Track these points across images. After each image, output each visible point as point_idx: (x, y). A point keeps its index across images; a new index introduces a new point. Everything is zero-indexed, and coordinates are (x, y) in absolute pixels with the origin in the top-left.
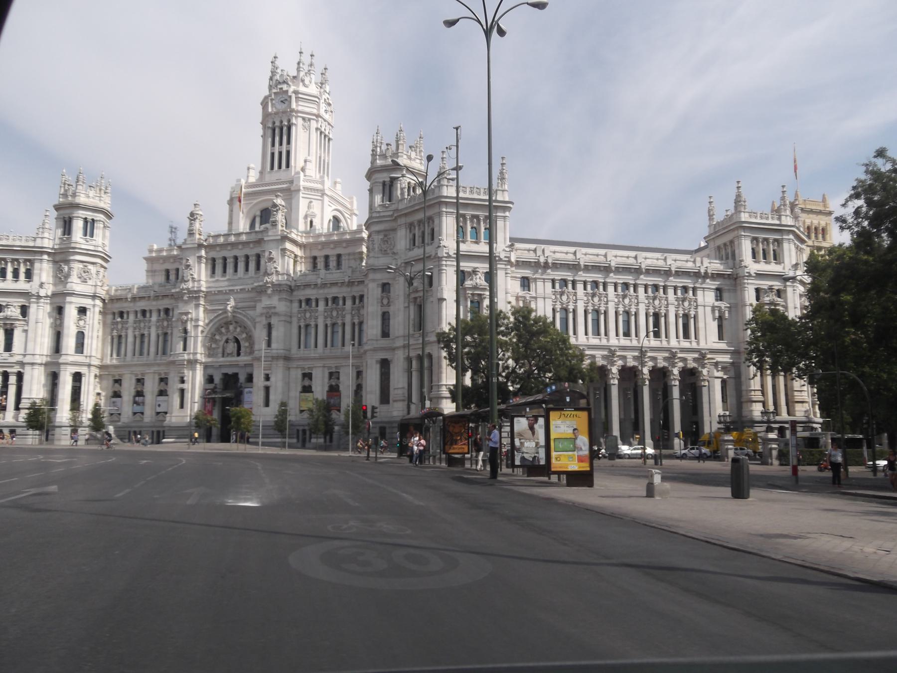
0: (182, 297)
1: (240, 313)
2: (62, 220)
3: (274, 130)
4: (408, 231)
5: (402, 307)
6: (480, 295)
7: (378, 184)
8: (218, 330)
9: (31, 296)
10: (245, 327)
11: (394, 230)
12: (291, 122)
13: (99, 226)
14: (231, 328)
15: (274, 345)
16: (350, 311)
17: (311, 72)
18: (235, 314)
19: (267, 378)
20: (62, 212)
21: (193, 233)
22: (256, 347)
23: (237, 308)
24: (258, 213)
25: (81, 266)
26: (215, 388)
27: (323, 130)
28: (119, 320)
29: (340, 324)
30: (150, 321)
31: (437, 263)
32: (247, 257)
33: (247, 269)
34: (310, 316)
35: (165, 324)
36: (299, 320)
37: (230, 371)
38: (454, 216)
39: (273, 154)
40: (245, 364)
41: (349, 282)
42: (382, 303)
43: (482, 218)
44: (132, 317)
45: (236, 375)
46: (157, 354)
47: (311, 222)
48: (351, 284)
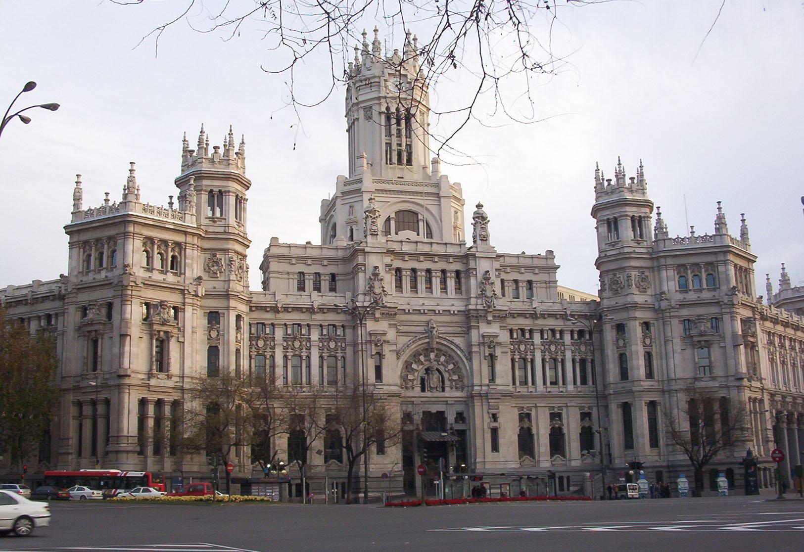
0: (373, 314)
1: (446, 339)
3: (388, 119)
5: (678, 348)
7: (628, 218)
8: (416, 356)
12: (413, 111)
14: (432, 356)
15: (498, 381)
18: (438, 340)
19: (495, 417)
21: (377, 235)
22: (476, 381)
24: (393, 215)
29: (560, 360)
30: (309, 340)
31: (728, 310)
33: (444, 288)
35: (332, 345)
36: (513, 352)
37: (434, 409)
39: (389, 145)
40: (455, 401)
42: (644, 342)
44: (279, 333)
45: (441, 414)
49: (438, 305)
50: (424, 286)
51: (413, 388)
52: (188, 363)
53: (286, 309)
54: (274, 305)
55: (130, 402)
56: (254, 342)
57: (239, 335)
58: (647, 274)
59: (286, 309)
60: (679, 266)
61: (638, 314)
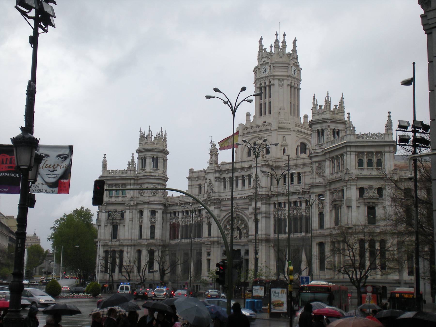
1: (240, 212)
2: (141, 159)
4: (331, 162)
6: (374, 202)
9: (126, 205)
11: (324, 161)
12: (271, 83)
13: (160, 161)
16: (305, 210)
17: (284, 47)
18: (237, 213)
20: (140, 154)
23: (239, 209)
27: (293, 84)
29: (298, 218)
31: (345, 184)
33: (243, 184)
34: (281, 213)
38: (356, 154)
39: (261, 104)
40: (244, 244)
41: (303, 192)
43: (375, 153)
44: (181, 215)
47: (284, 150)
48: (304, 193)
49: (239, 194)
52: (127, 234)
53: (182, 204)
55: (100, 252)
57: (153, 220)
58: (323, 164)
60: (333, 158)
61: (316, 190)
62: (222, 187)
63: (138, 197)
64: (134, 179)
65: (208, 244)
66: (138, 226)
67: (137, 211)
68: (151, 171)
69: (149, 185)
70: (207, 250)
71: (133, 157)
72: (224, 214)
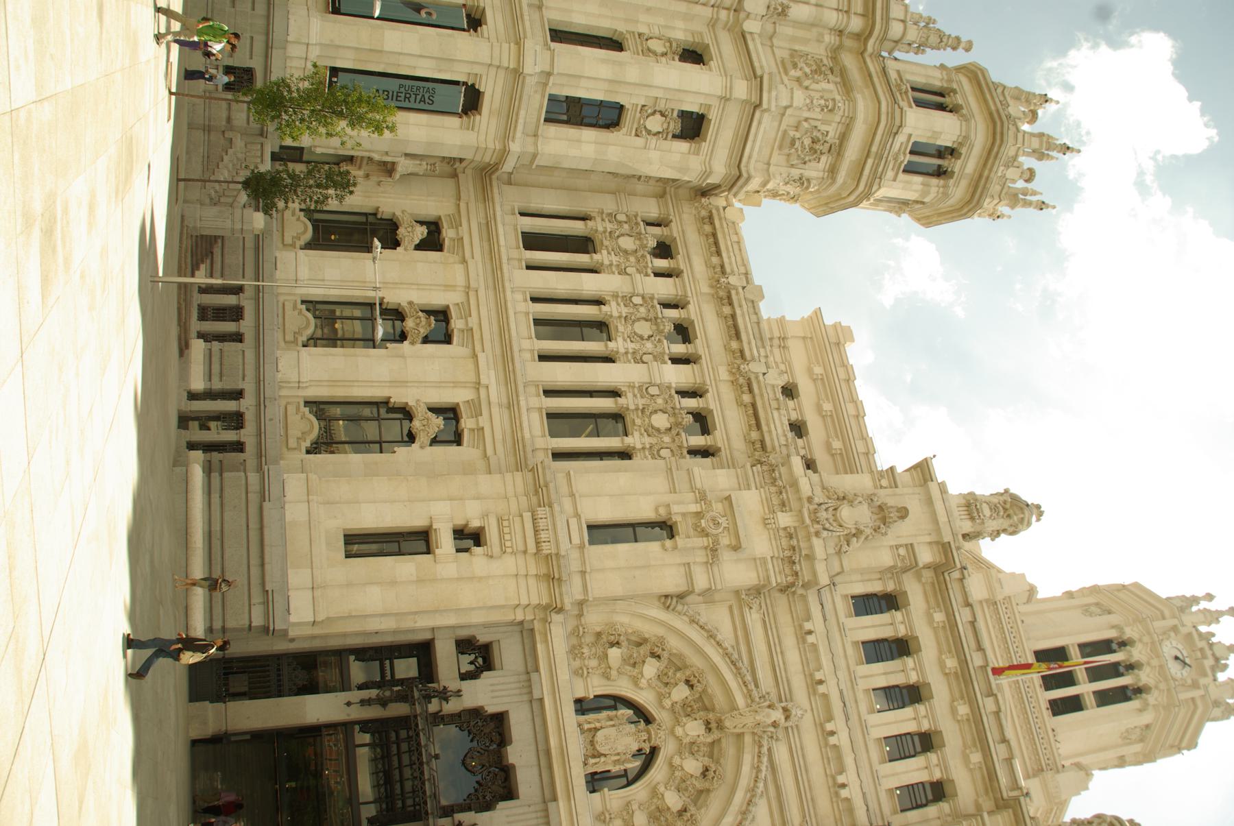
10: (708, 791)
14: (693, 729)
18: (748, 739)
23: (769, 750)
25: (832, 131)
26: (444, 695)
28: (652, 243)
30: (658, 358)
32: (926, 742)
35: (661, 421)
37: (519, 754)
44: (664, 288)
46: (549, 393)
50: (882, 682)
51: (578, 673)
53: (725, 298)
54: (728, 270)
56: (626, 226)
57: (655, 123)
59: (725, 298)
62: (860, 589)
63: (772, 47)
64: (862, 37)
65: (543, 535)
66: (621, 27)
67: (704, 29)
68: (901, 138)
69: (837, 119)
70: (500, 520)
71: (956, 44)
72: (726, 632)
